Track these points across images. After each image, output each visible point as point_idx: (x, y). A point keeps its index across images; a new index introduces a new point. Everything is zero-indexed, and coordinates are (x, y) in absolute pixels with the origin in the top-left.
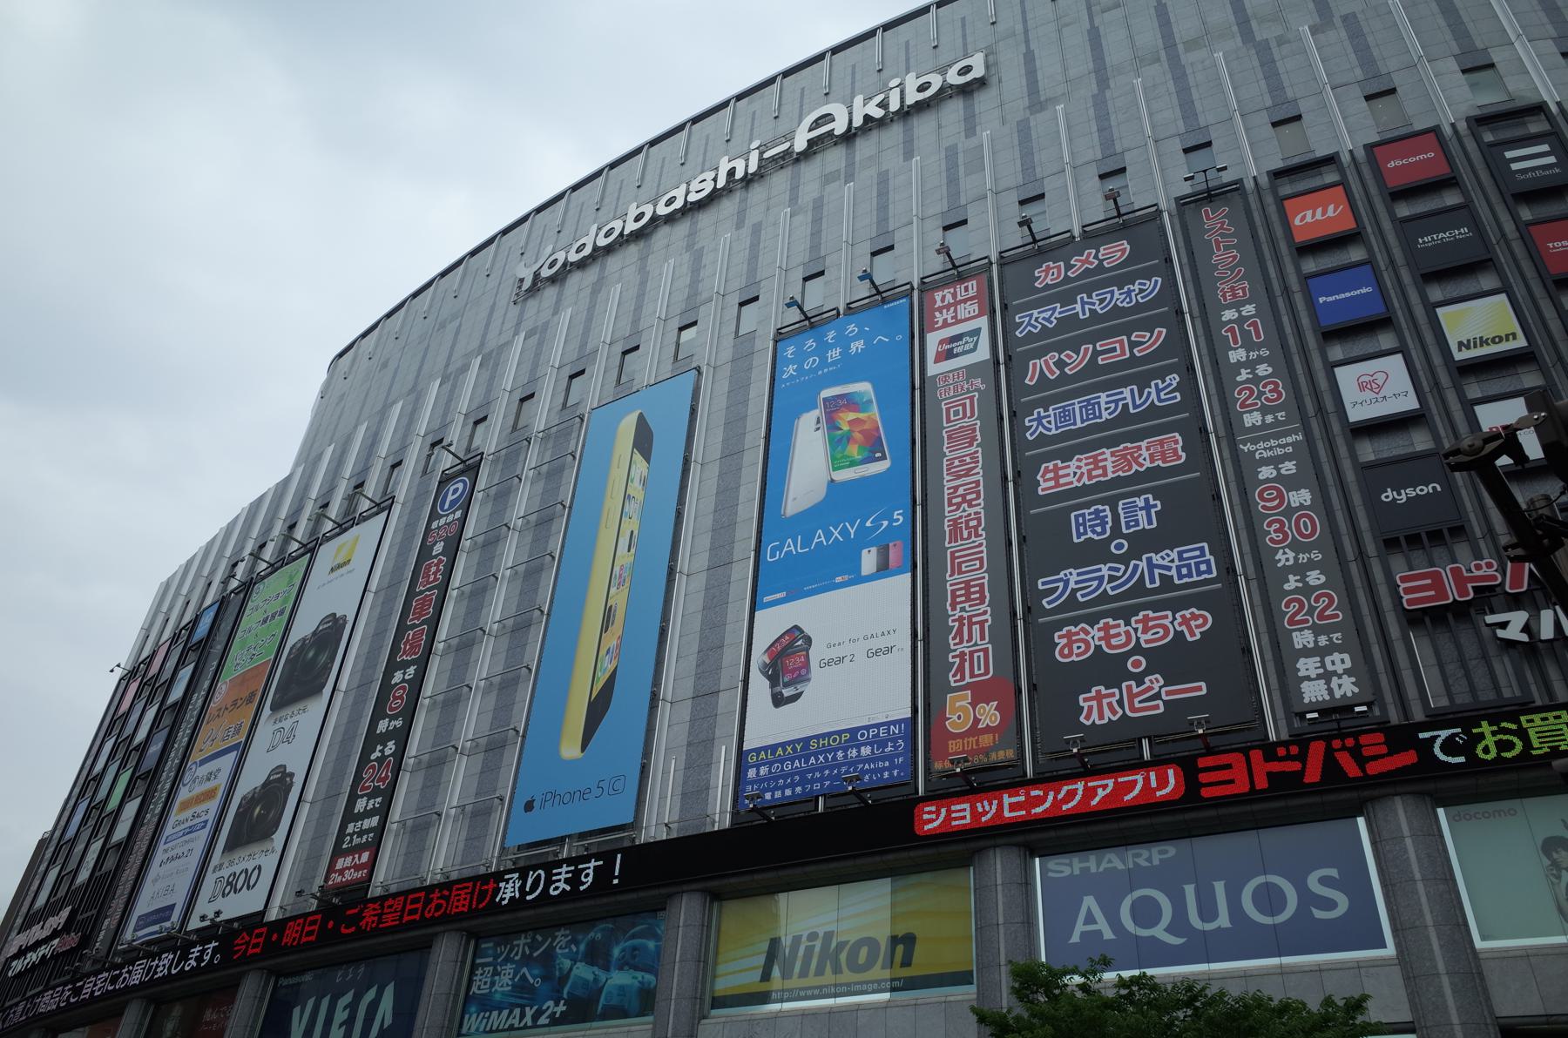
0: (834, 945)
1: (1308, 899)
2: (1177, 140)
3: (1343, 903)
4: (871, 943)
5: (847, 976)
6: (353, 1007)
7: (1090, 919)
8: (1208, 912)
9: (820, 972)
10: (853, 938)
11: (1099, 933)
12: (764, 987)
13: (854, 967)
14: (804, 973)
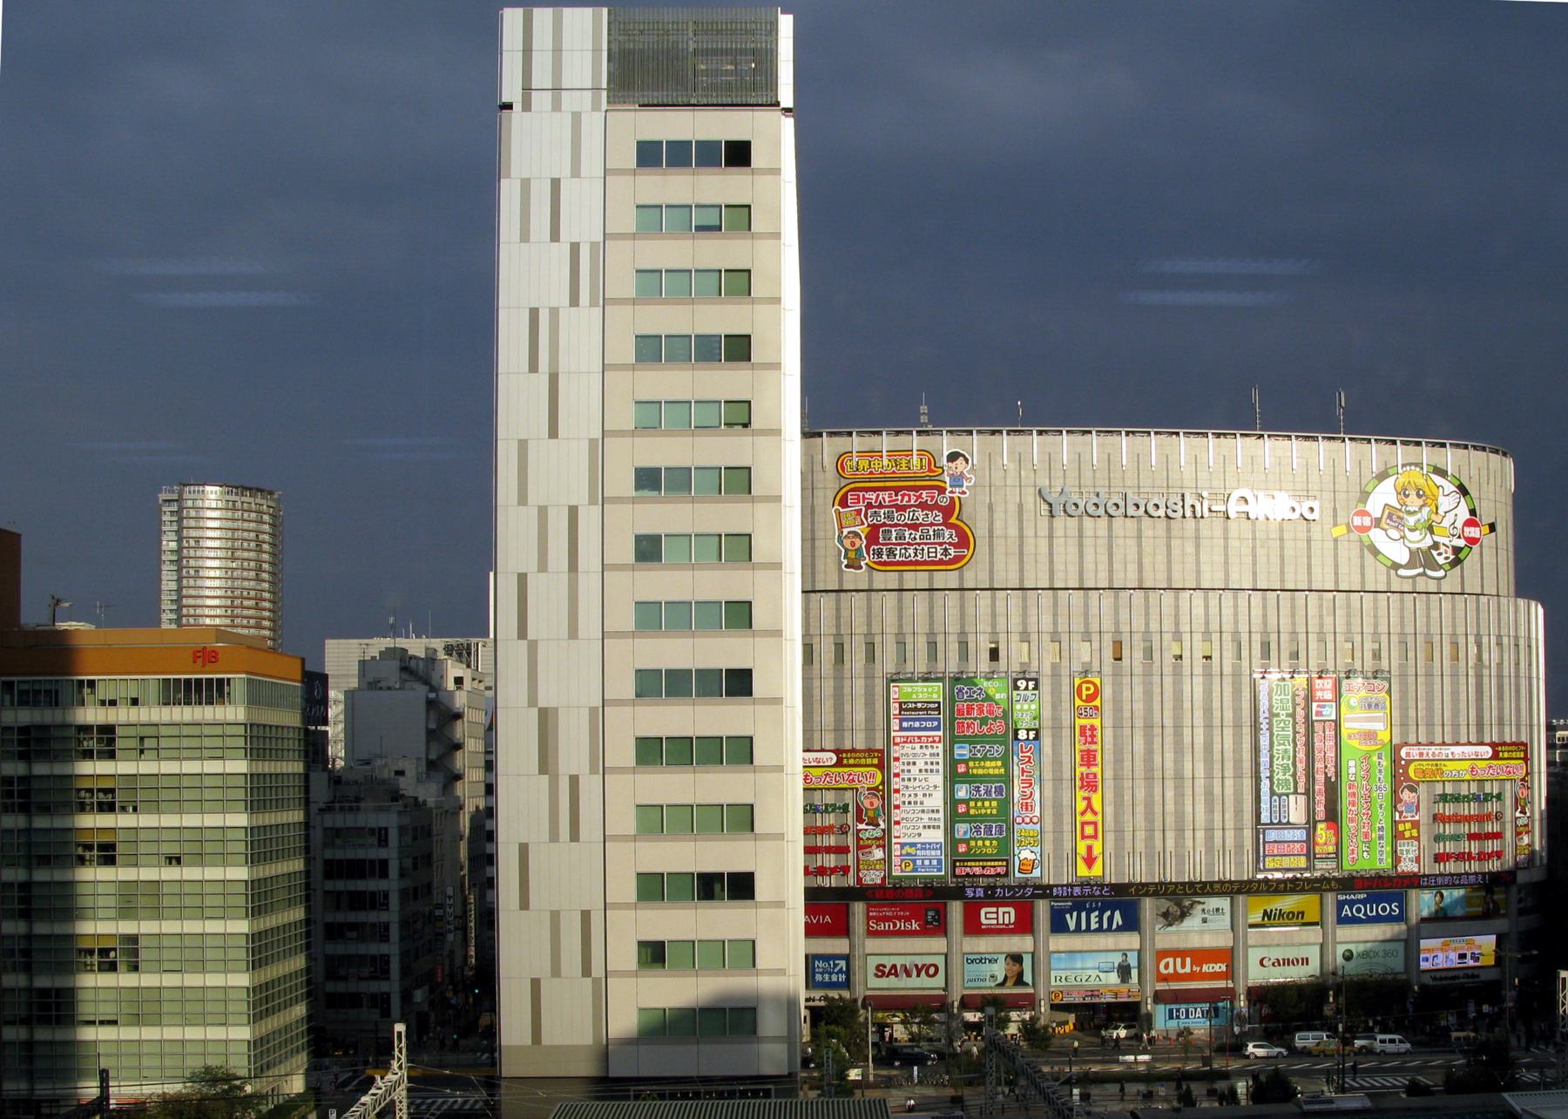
1: (1391, 909)
4: (1293, 913)
5: (1286, 921)
8: (1371, 911)
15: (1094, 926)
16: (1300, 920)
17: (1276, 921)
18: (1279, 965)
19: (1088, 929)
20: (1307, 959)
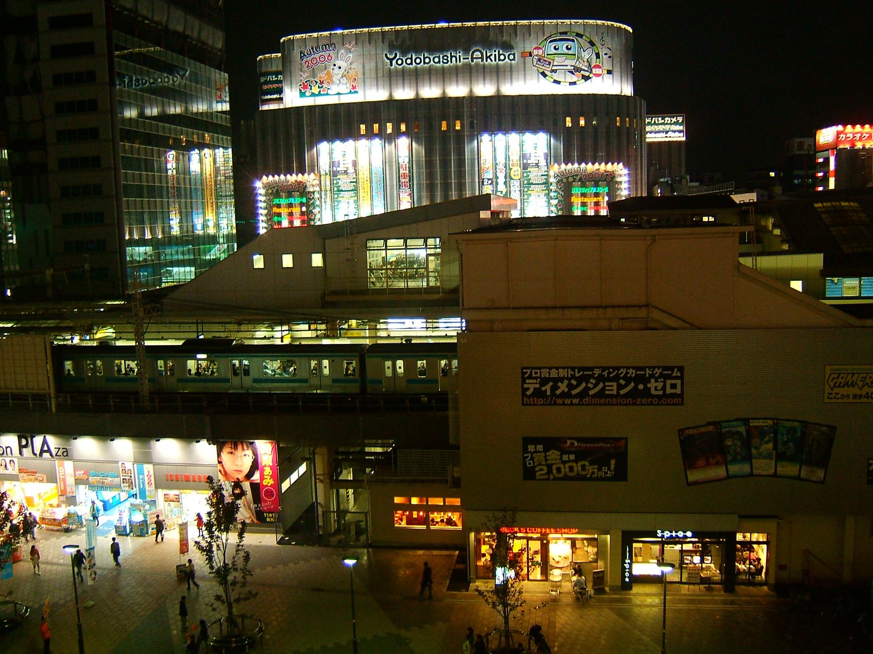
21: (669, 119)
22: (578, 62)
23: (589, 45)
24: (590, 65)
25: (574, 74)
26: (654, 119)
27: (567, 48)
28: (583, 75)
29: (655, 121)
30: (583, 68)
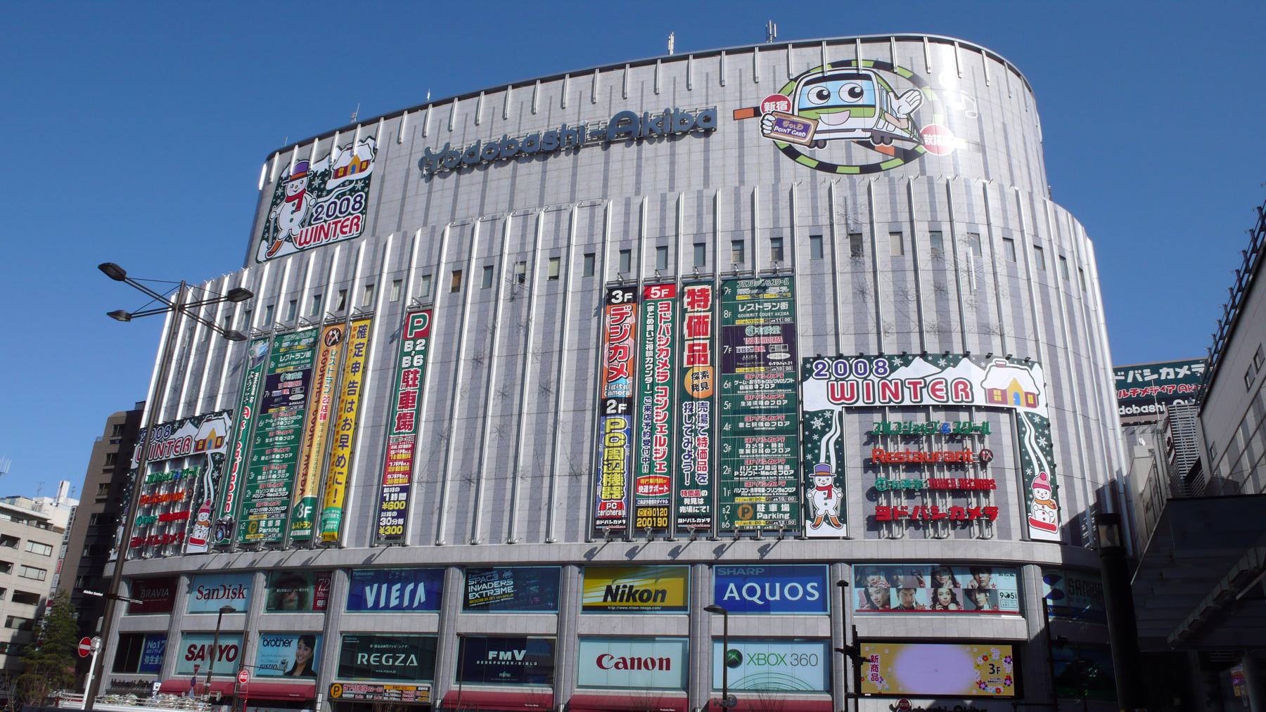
0: (634, 590)
1: (806, 593)
2: (808, 229)
3: (817, 595)
5: (639, 603)
6: (402, 590)
7: (732, 592)
9: (628, 600)
10: (641, 589)
11: (734, 597)
12: (605, 604)
13: (641, 599)
14: (621, 600)
15: (394, 602)
16: (658, 603)
17: (624, 603)
18: (626, 667)
19: (387, 608)
20: (668, 660)
21: (1171, 371)
22: (882, 122)
23: (910, 85)
24: (915, 126)
25: (872, 148)
26: (1131, 373)
27: (852, 93)
28: (896, 149)
29: (1134, 378)
30: (898, 132)
